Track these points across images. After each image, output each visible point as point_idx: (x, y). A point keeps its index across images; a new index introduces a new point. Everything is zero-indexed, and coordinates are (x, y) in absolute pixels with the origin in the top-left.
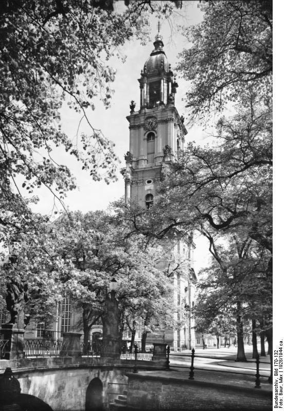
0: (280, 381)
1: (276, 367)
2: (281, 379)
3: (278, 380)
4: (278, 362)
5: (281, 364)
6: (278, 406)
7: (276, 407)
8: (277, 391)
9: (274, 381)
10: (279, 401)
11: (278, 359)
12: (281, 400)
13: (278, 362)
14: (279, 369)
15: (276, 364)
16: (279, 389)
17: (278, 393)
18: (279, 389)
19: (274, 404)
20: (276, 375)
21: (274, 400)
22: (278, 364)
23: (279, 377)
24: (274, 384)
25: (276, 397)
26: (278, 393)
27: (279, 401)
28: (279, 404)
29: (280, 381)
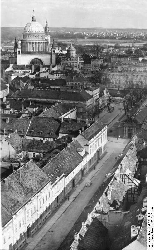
0: (151, 232)
1: (150, 223)
2: (152, 230)
3: (150, 231)
4: (150, 220)
5: (152, 221)
6: (150, 247)
7: (149, 248)
8: (150, 238)
9: (148, 232)
10: (151, 244)
11: (150, 218)
12: (152, 243)
13: (150, 220)
14: (151, 225)
15: (149, 222)
16: (151, 237)
17: (151, 239)
18: (151, 237)
19: (148, 246)
20: (149, 228)
21: (148, 244)
22: (150, 222)
23: (151, 229)
24: (148, 234)
25: (149, 241)
26: (151, 239)
27: (151, 244)
28: (151, 246)
29: (151, 232)
